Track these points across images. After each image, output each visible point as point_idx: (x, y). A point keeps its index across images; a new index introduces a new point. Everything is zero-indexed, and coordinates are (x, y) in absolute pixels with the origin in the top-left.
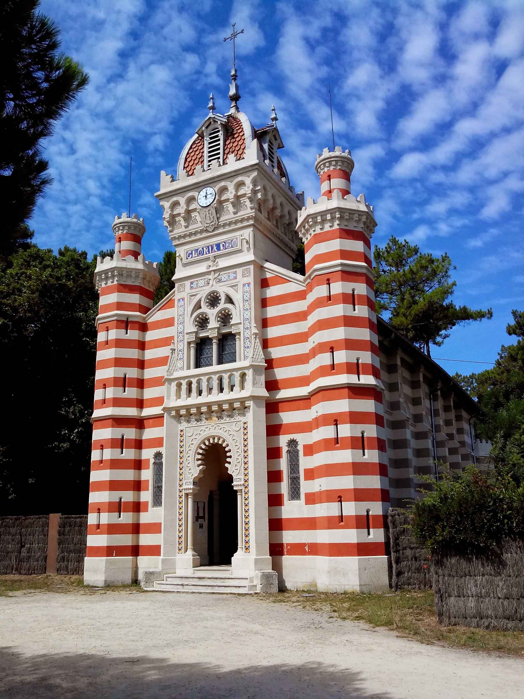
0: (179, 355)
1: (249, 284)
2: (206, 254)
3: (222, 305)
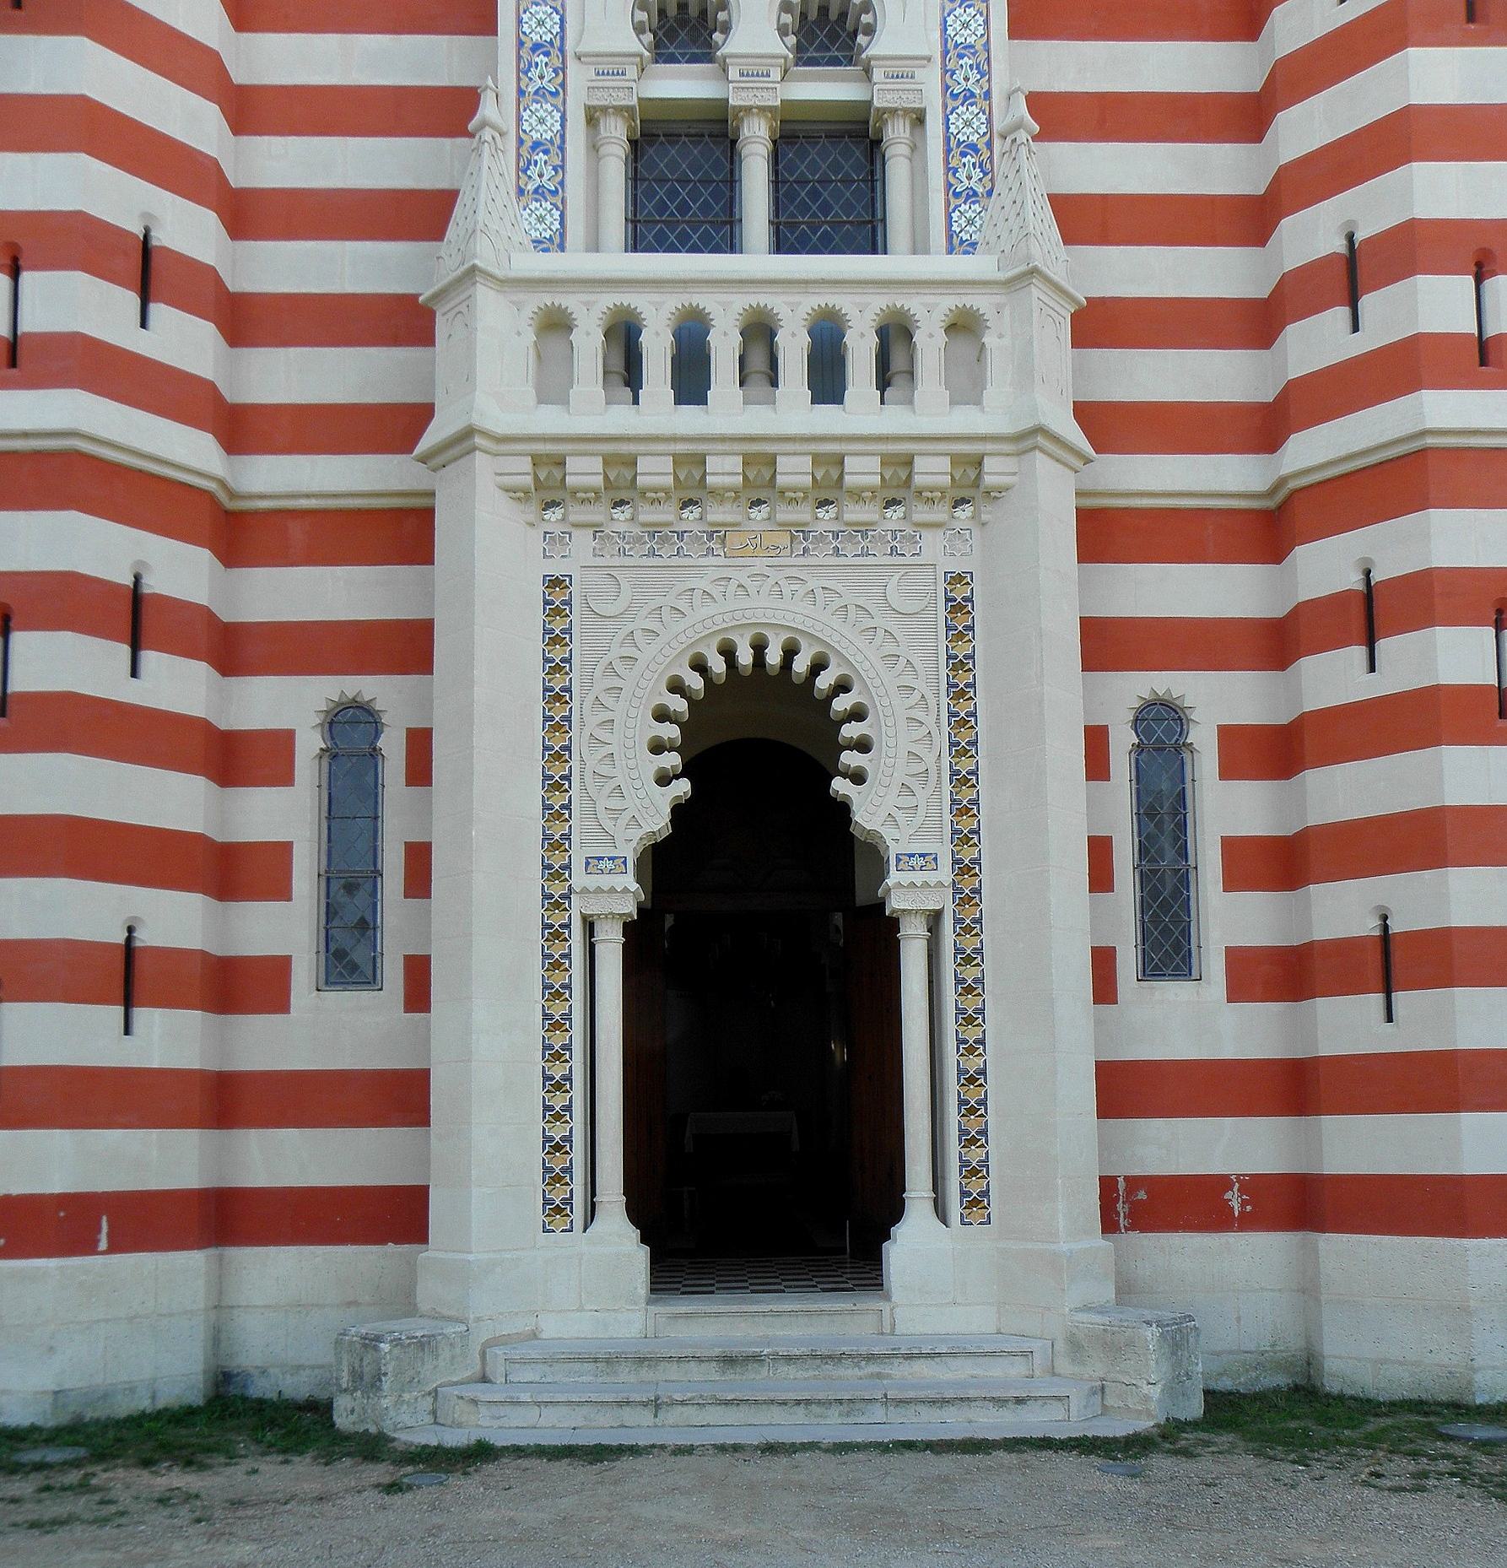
0: (533, 171)
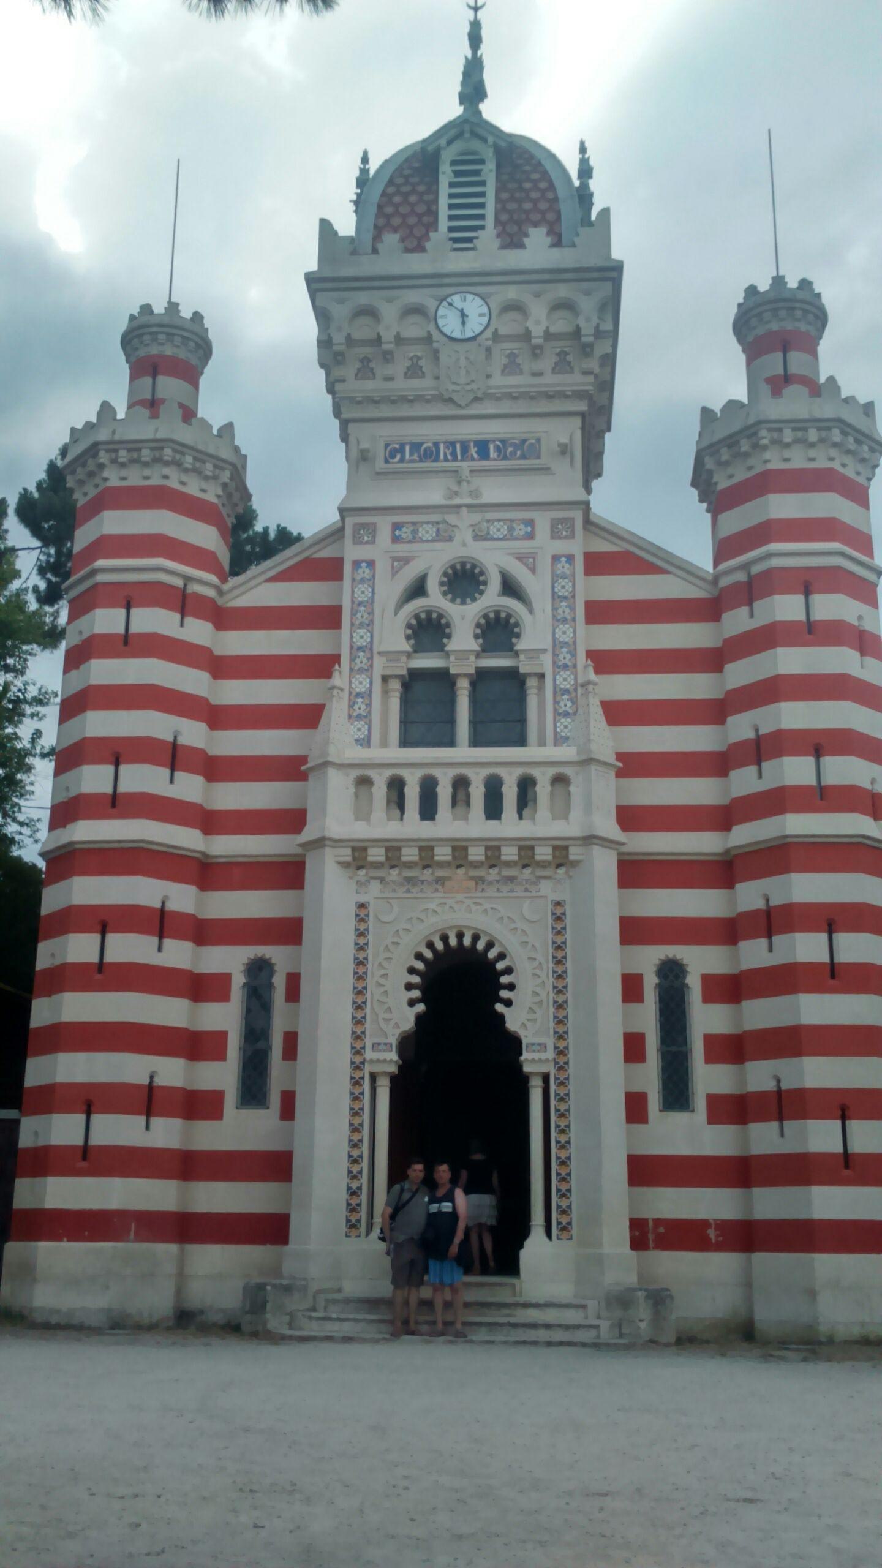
0: (356, 707)
1: (570, 558)
2: (446, 460)
3: (491, 598)
